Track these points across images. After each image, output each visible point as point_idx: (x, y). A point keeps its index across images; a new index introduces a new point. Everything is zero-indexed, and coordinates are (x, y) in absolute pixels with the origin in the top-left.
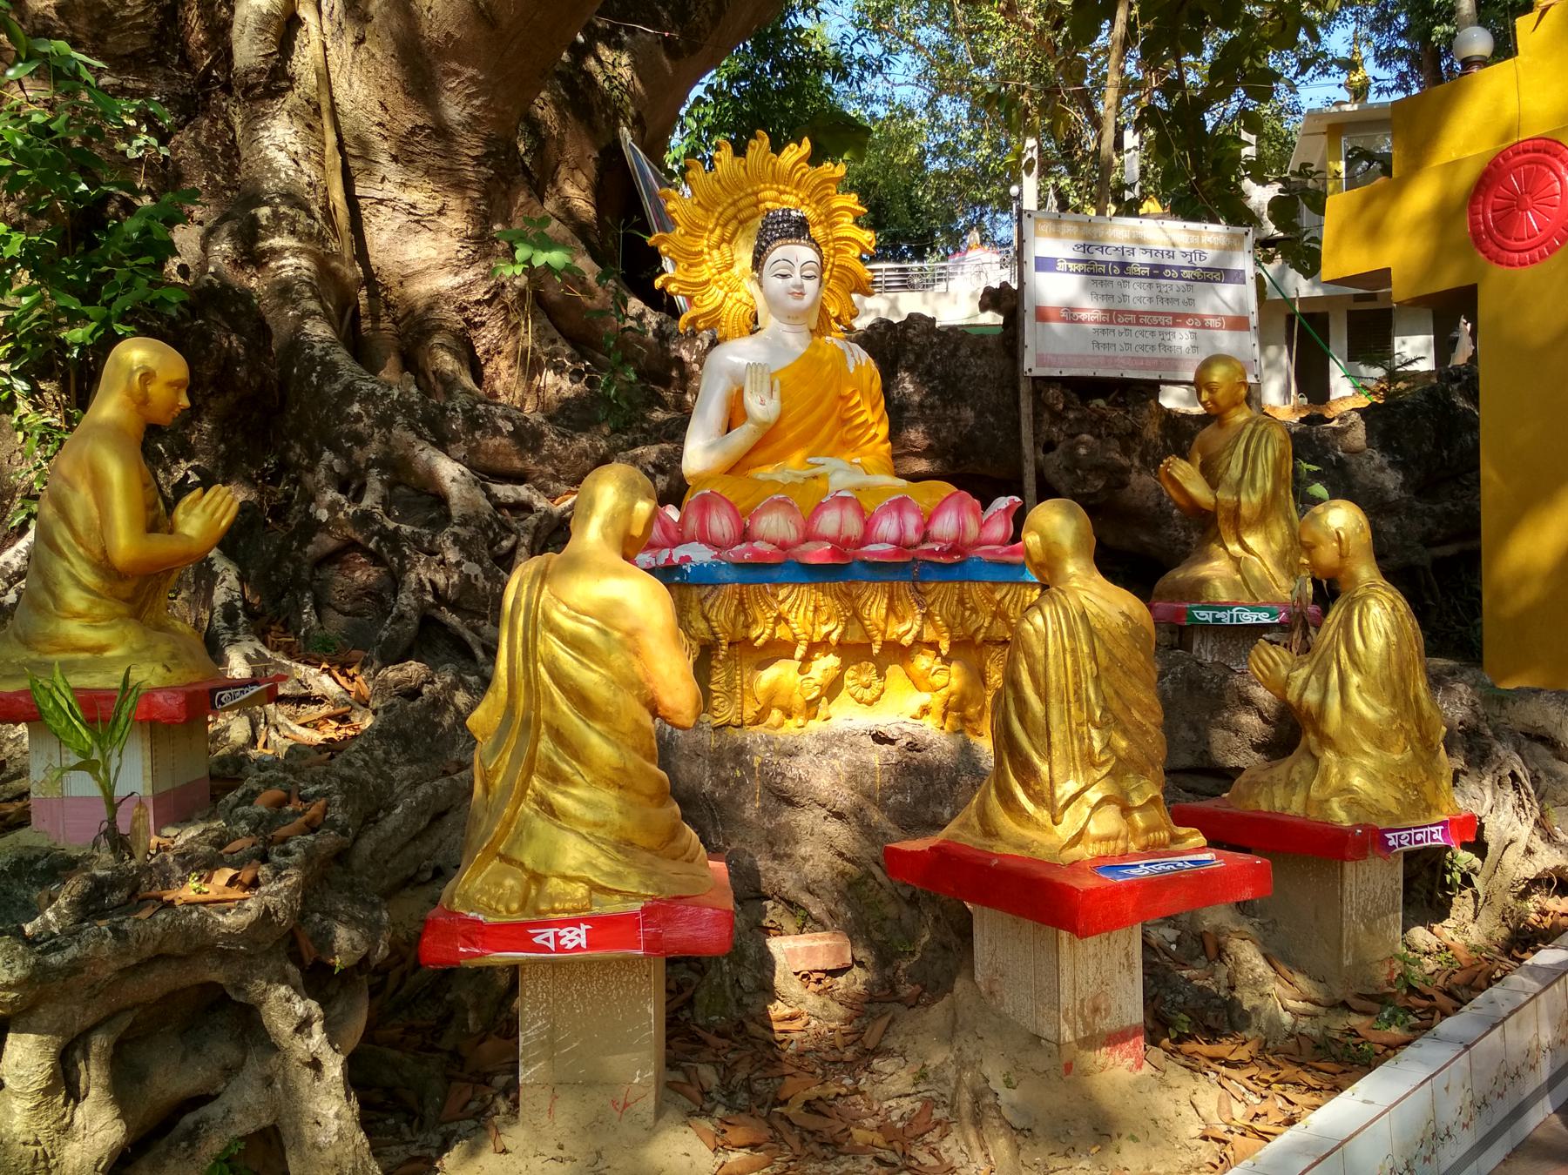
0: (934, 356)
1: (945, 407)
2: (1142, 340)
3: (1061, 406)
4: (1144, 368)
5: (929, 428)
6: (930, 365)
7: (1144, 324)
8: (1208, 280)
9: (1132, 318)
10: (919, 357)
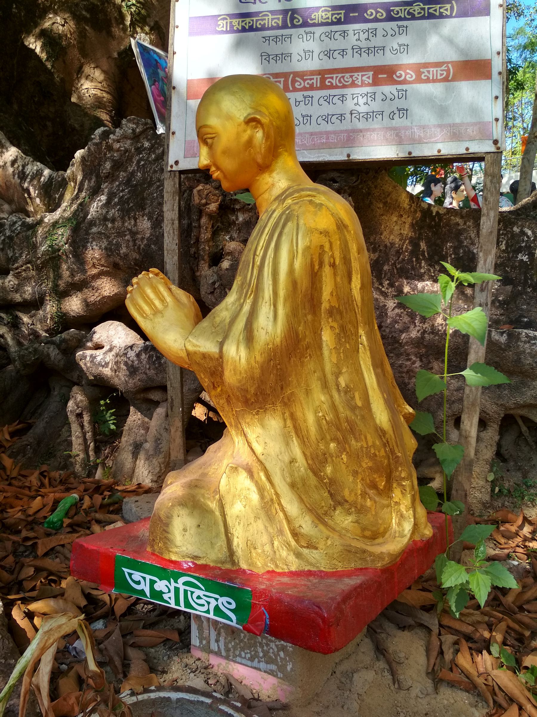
0: (138, 162)
1: (123, 218)
2: (327, 109)
3: (213, 207)
4: (329, 146)
5: (110, 243)
6: (133, 174)
7: (332, 87)
8: (431, 16)
9: (316, 80)
10: (118, 166)
